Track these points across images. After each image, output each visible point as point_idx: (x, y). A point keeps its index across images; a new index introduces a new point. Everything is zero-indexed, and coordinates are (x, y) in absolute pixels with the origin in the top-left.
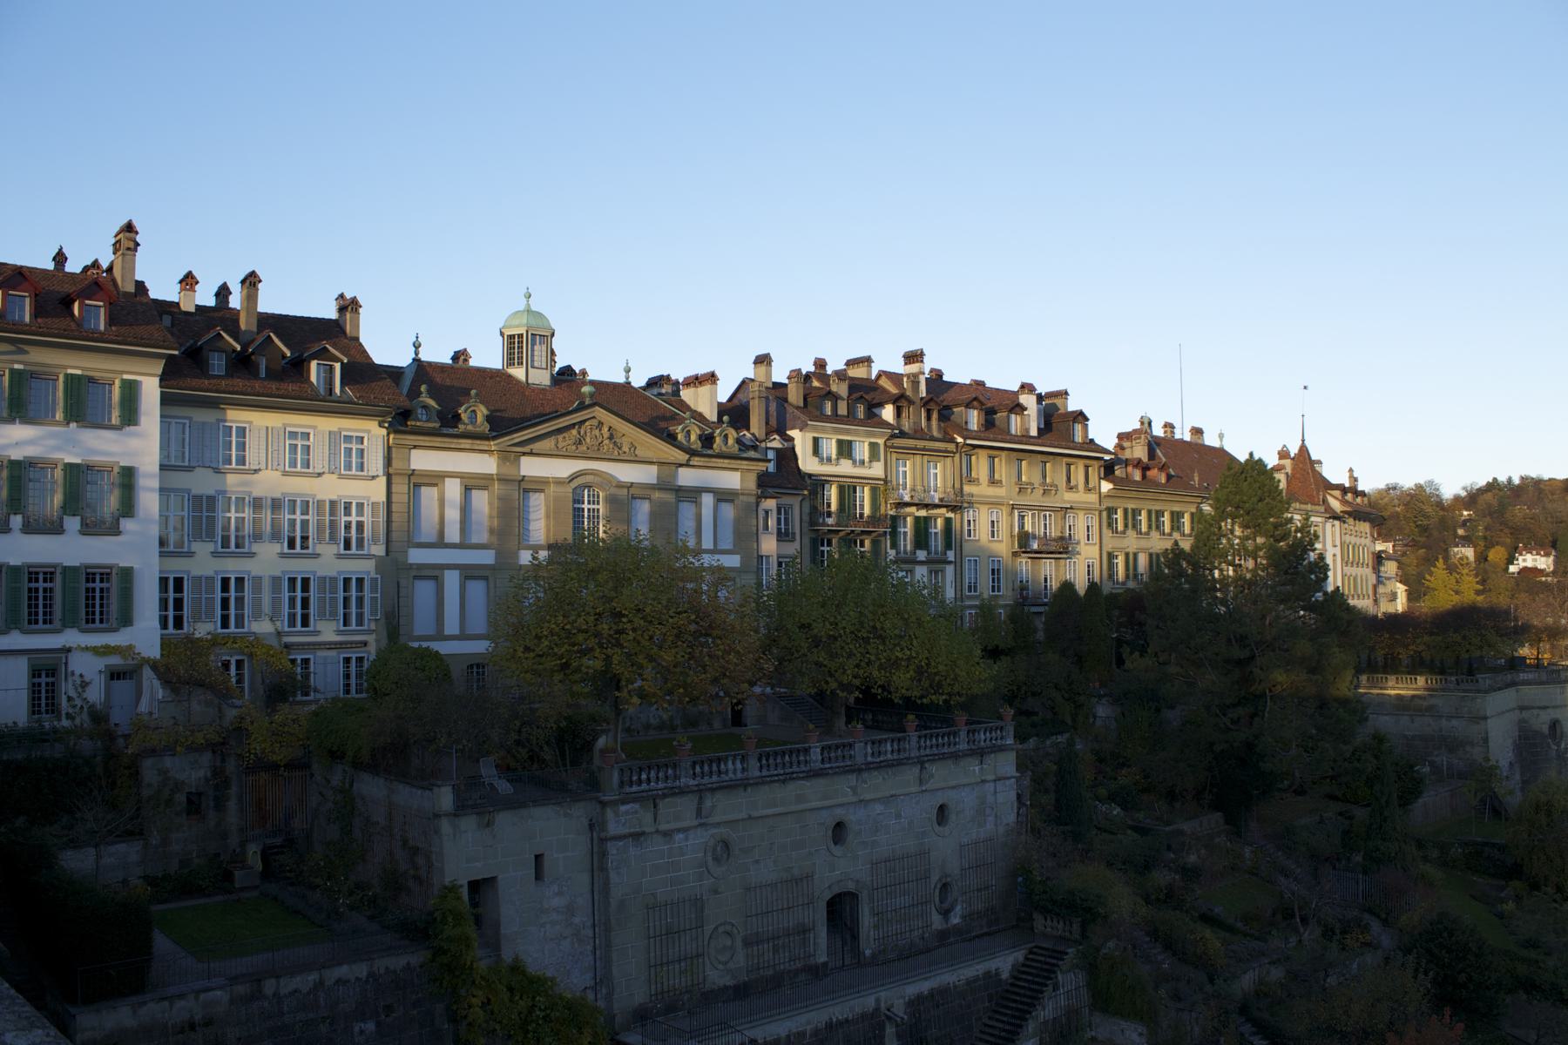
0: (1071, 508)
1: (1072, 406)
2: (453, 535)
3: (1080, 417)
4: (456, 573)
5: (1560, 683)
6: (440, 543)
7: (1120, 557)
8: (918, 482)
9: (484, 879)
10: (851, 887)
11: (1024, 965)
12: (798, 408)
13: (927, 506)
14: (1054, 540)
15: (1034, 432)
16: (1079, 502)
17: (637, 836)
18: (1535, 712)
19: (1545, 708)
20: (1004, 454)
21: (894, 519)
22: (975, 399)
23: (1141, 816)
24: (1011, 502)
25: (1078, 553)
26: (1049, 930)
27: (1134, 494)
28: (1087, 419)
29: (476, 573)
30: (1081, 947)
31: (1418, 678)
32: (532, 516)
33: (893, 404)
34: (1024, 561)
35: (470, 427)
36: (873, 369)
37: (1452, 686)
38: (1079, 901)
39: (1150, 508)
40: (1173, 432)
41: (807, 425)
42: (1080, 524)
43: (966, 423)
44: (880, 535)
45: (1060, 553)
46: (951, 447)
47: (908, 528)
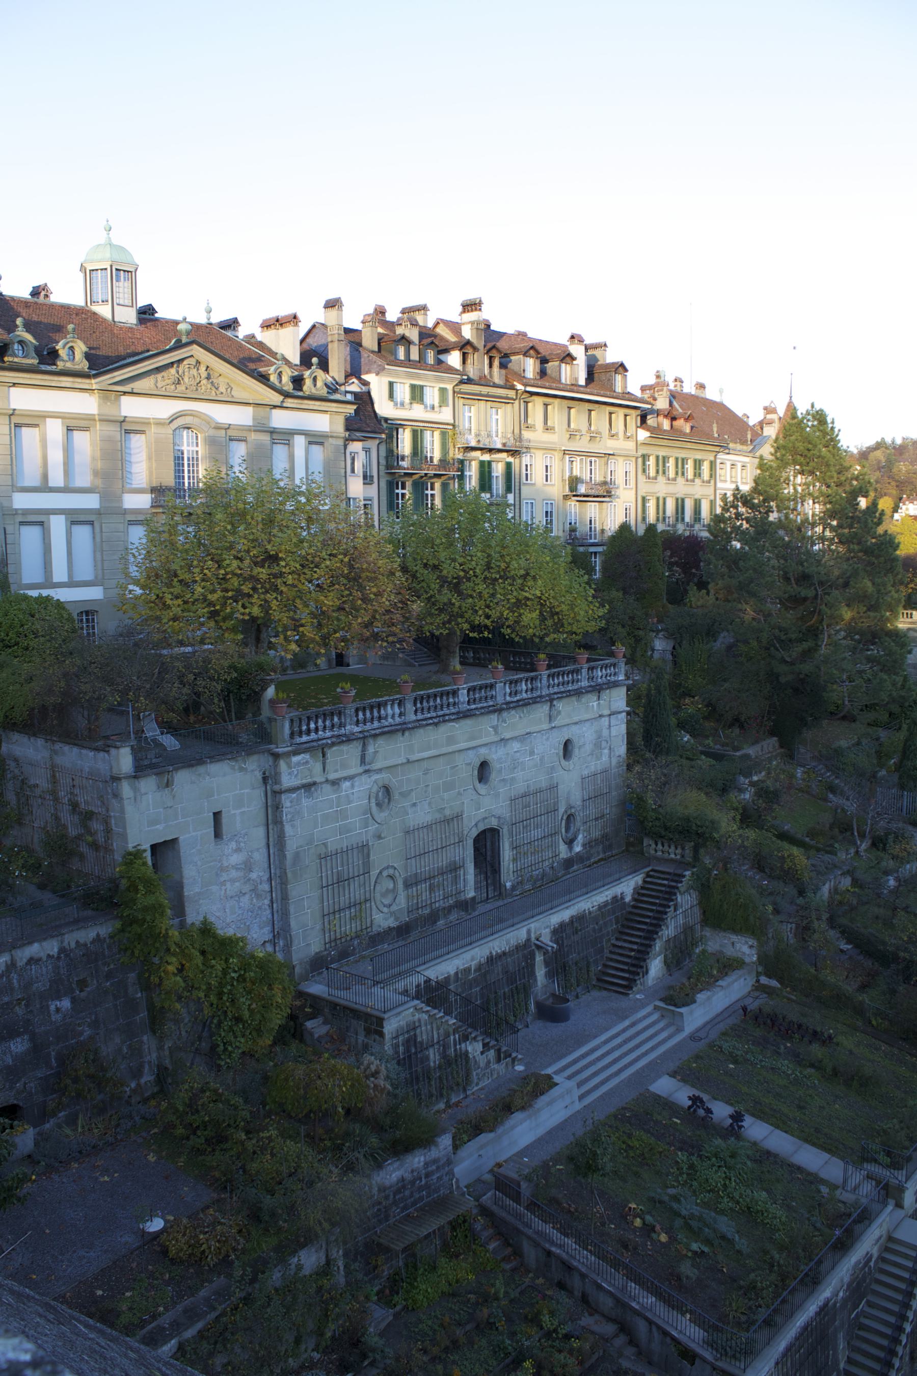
0: (613, 455)
1: (611, 357)
2: (57, 478)
3: (621, 368)
4: (62, 518)
6: (44, 487)
7: (651, 501)
8: (483, 428)
9: (165, 842)
10: (494, 823)
11: (642, 888)
12: (373, 352)
13: (491, 451)
14: (599, 484)
15: (582, 382)
16: (620, 449)
17: (309, 787)
20: (557, 401)
21: (462, 462)
22: (532, 348)
23: (710, 741)
24: (563, 448)
25: (618, 497)
26: (660, 853)
27: (665, 443)
28: (626, 370)
29: (82, 518)
30: (695, 870)
32: (134, 459)
33: (460, 350)
34: (573, 503)
35: (69, 365)
36: (429, 317)
38: (694, 828)
39: (678, 455)
40: (682, 386)
41: (384, 369)
42: (621, 470)
43: (524, 371)
44: (449, 479)
45: (604, 497)
46: (511, 393)
47: (473, 473)
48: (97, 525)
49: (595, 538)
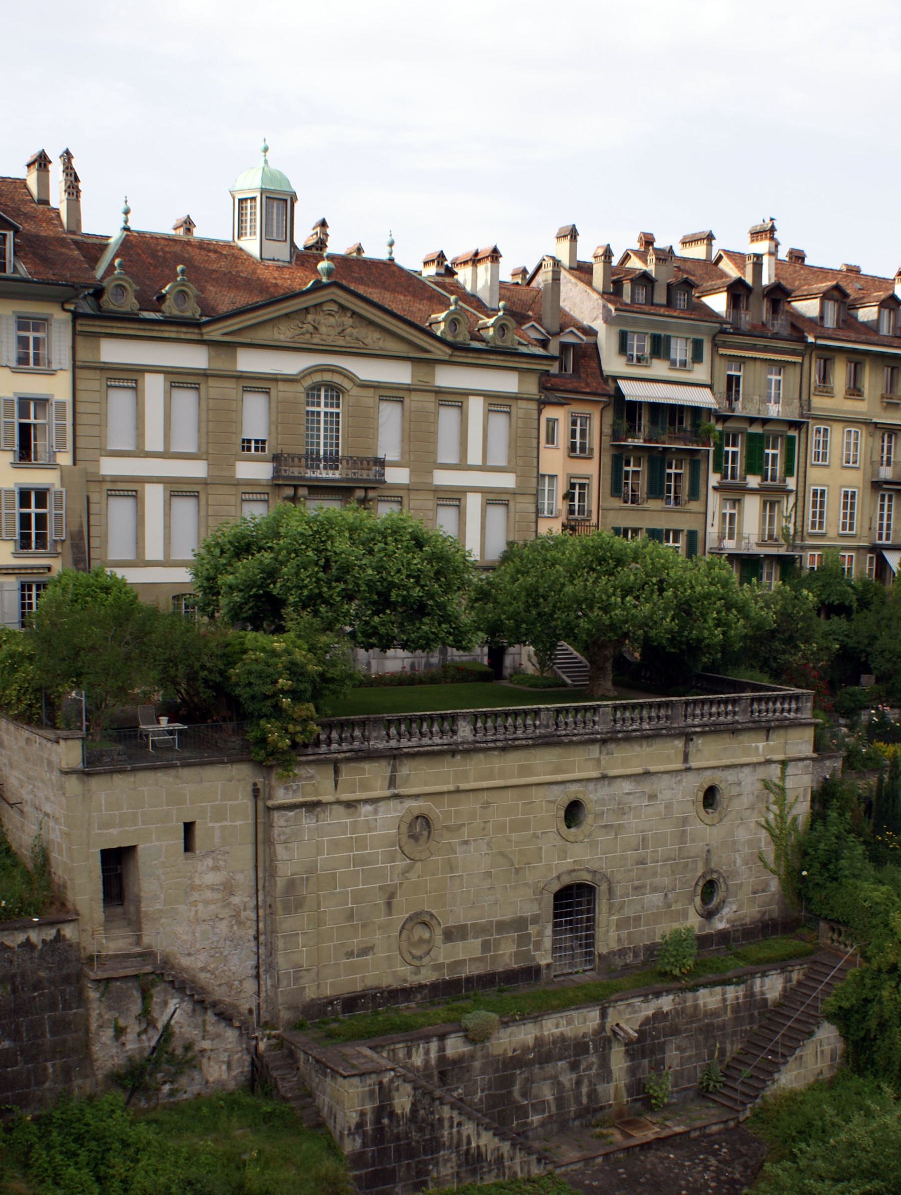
17: (312, 806)
48: (202, 497)
49: (888, 538)
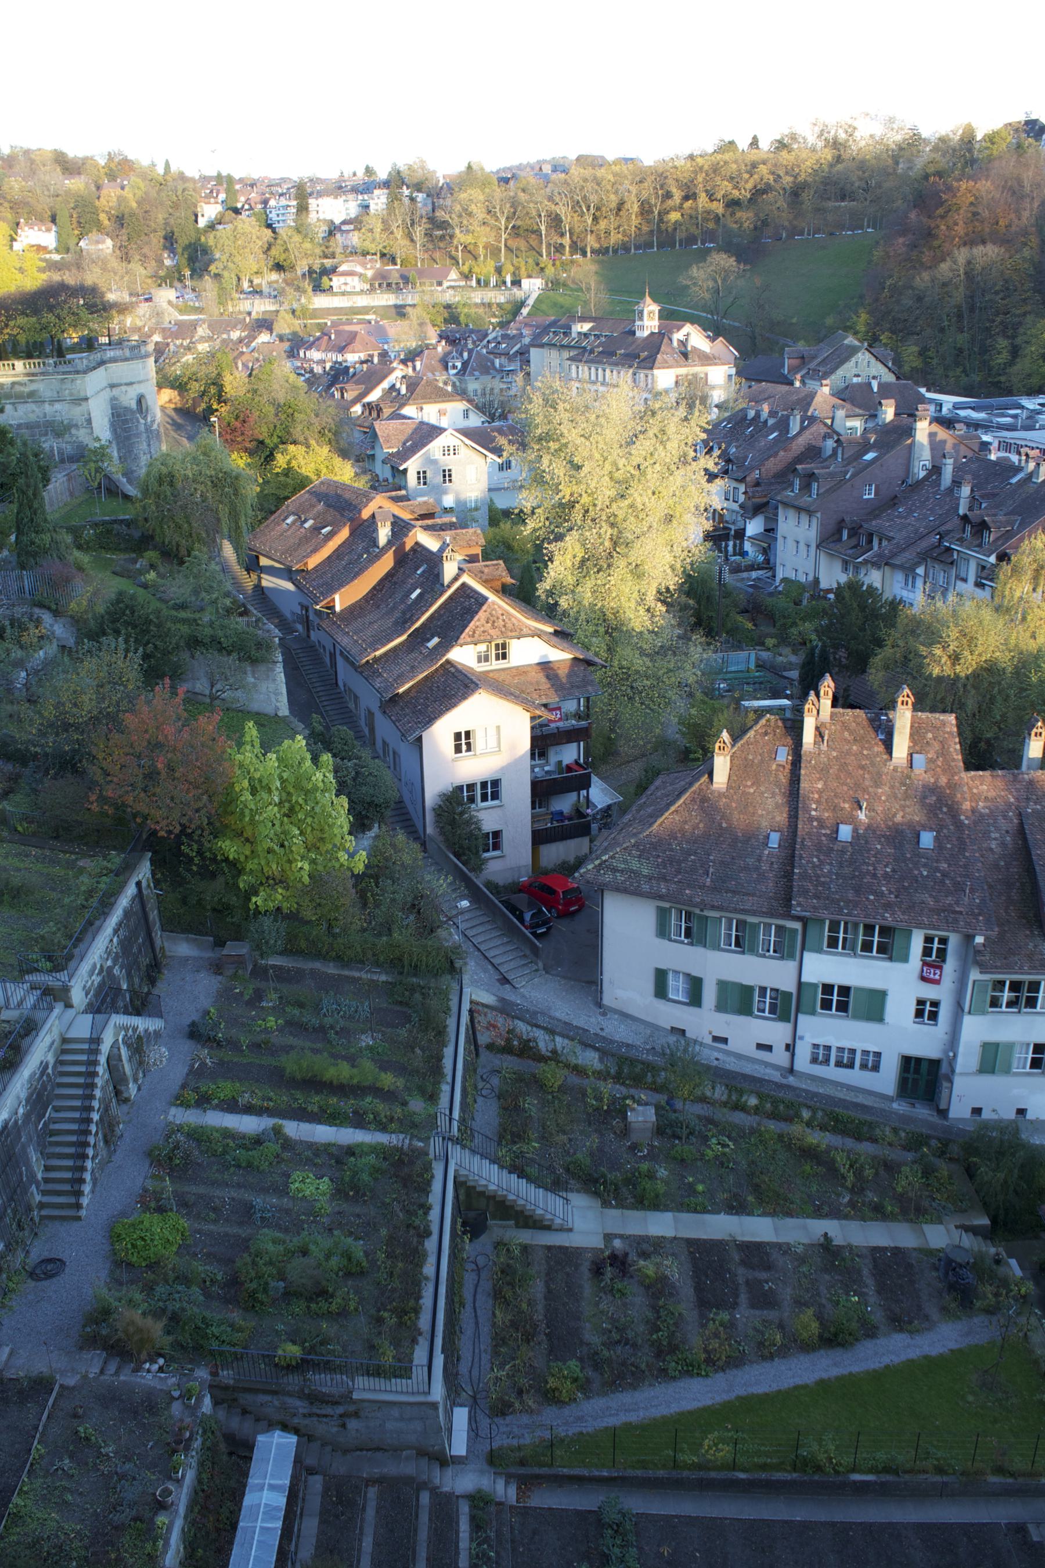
5: (142, 358)
18: (124, 388)
19: (131, 384)
31: (16, 363)
37: (50, 369)
